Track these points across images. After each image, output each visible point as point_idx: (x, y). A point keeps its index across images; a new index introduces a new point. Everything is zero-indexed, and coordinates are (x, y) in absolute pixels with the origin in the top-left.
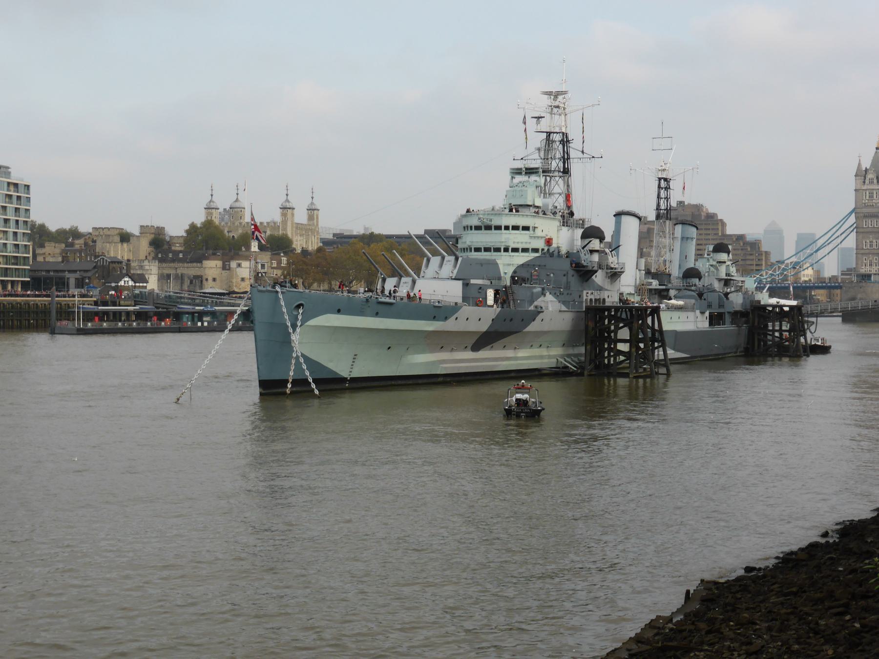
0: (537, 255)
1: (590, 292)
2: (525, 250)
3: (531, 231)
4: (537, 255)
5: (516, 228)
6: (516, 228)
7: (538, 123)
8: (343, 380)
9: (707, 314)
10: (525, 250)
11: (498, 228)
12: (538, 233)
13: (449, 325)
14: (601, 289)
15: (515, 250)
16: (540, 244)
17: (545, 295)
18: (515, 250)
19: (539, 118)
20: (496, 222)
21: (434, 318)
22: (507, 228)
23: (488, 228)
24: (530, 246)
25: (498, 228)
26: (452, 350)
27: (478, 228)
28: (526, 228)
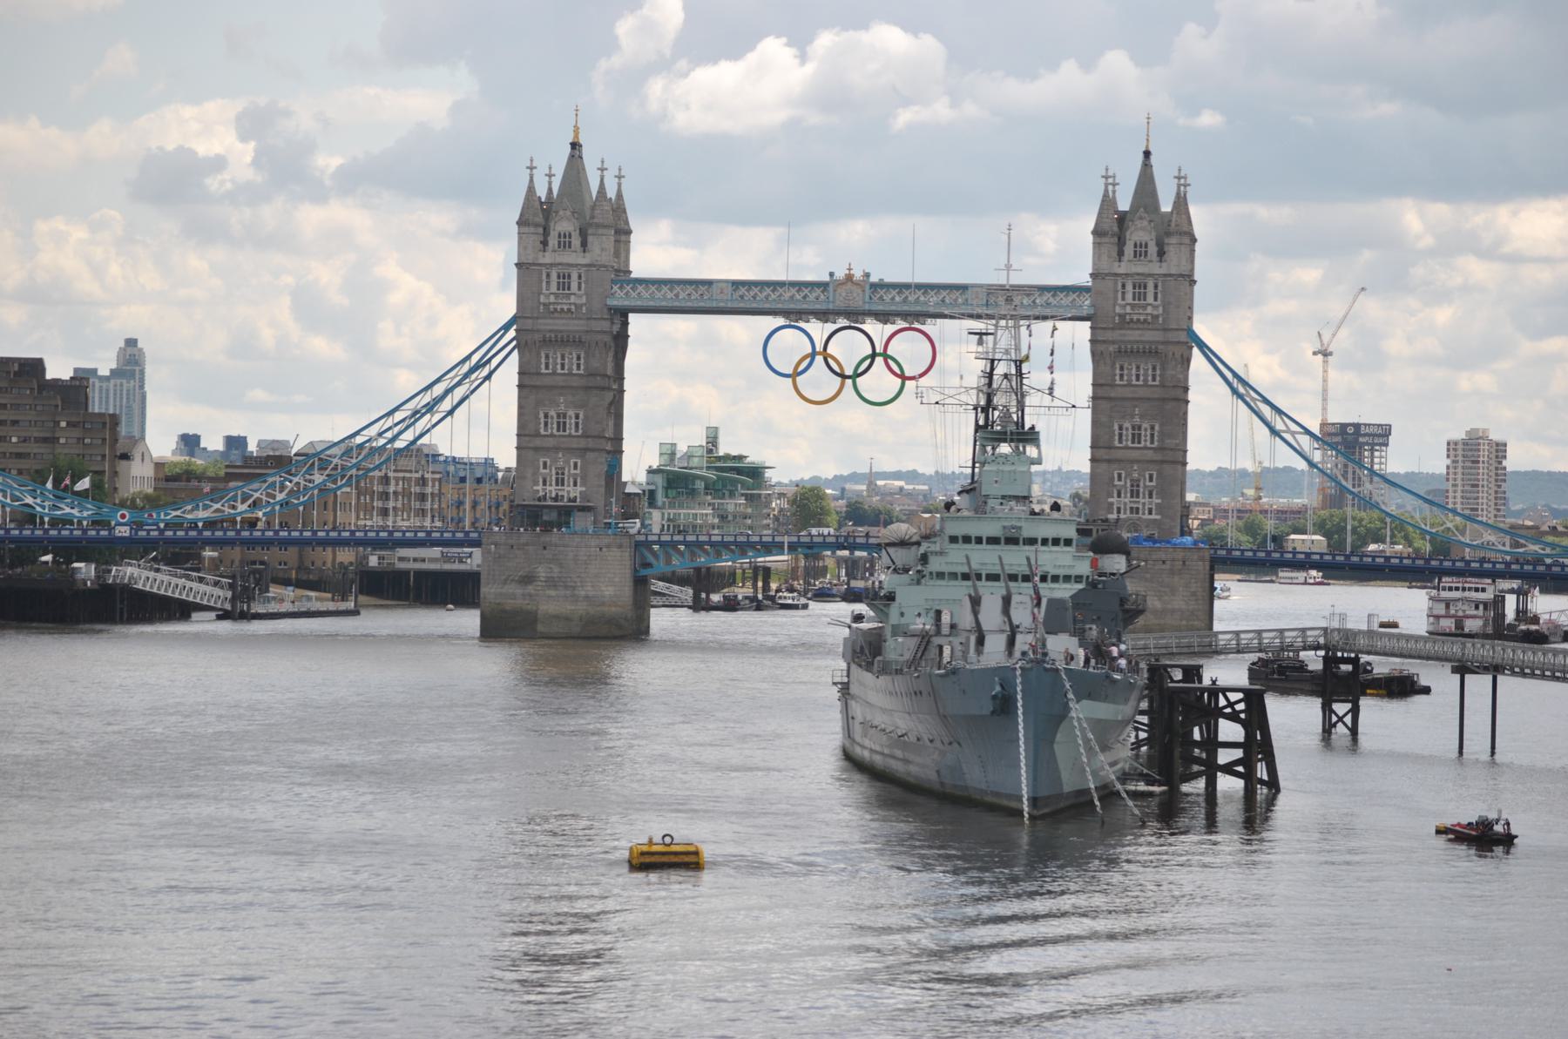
0: (1080, 586)
2: (1067, 578)
4: (1080, 586)
5: (1056, 542)
6: (1056, 542)
7: (980, 342)
10: (1067, 578)
11: (1031, 541)
15: (1055, 579)
19: (981, 334)
20: (1029, 530)
22: (1045, 542)
23: (1012, 541)
24: (1074, 572)
25: (1031, 541)
27: (993, 541)
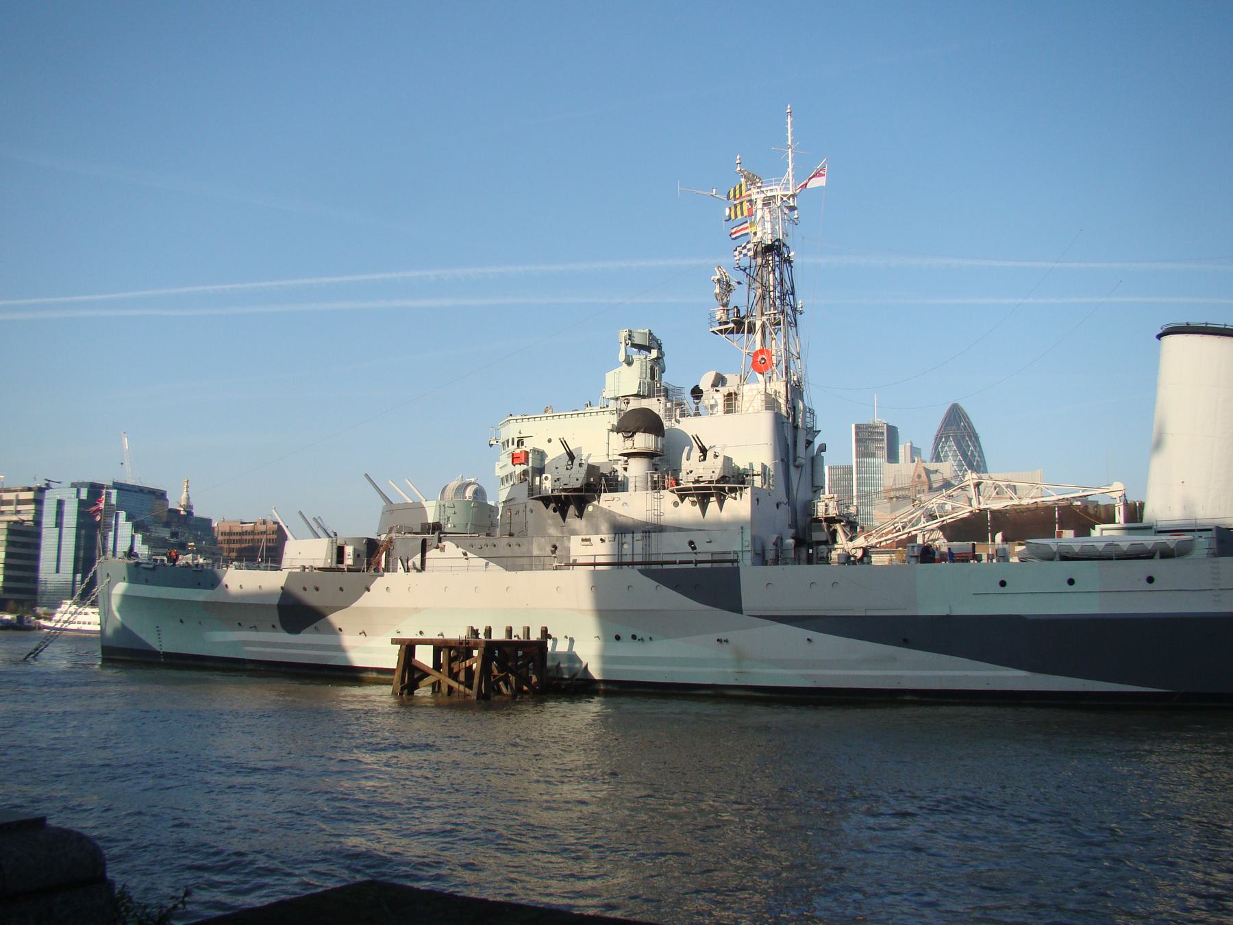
8: (157, 653)
17: (443, 549)
26: (255, 628)
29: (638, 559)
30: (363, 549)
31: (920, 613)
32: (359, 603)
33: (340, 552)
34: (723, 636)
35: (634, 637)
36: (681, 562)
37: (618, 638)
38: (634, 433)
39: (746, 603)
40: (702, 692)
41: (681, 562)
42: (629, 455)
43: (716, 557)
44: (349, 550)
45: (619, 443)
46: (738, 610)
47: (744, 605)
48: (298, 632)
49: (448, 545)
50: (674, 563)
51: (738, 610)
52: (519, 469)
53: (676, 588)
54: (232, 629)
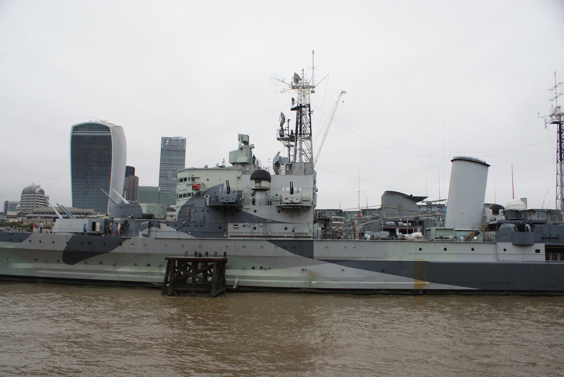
0: (190, 198)
1: (241, 225)
2: (185, 195)
3: (188, 182)
9: (541, 246)
10: (185, 195)
12: (196, 180)
13: (25, 245)
14: (264, 221)
15: (181, 196)
16: (190, 190)
17: (159, 227)
18: (181, 196)
21: (11, 240)
26: (46, 261)
28: (185, 179)
29: (261, 235)
30: (103, 224)
31: (389, 259)
32: (115, 251)
33: (94, 224)
34: (304, 268)
35: (261, 268)
36: (287, 237)
37: (253, 268)
38: (261, 181)
39: (315, 254)
40: (293, 291)
41: (287, 237)
42: (256, 190)
43: (297, 235)
44: (98, 224)
45: (253, 185)
46: (312, 257)
47: (315, 255)
48: (74, 264)
49: (163, 226)
50: (284, 237)
51: (312, 257)
52: (195, 192)
53: (285, 248)
54: (29, 262)
